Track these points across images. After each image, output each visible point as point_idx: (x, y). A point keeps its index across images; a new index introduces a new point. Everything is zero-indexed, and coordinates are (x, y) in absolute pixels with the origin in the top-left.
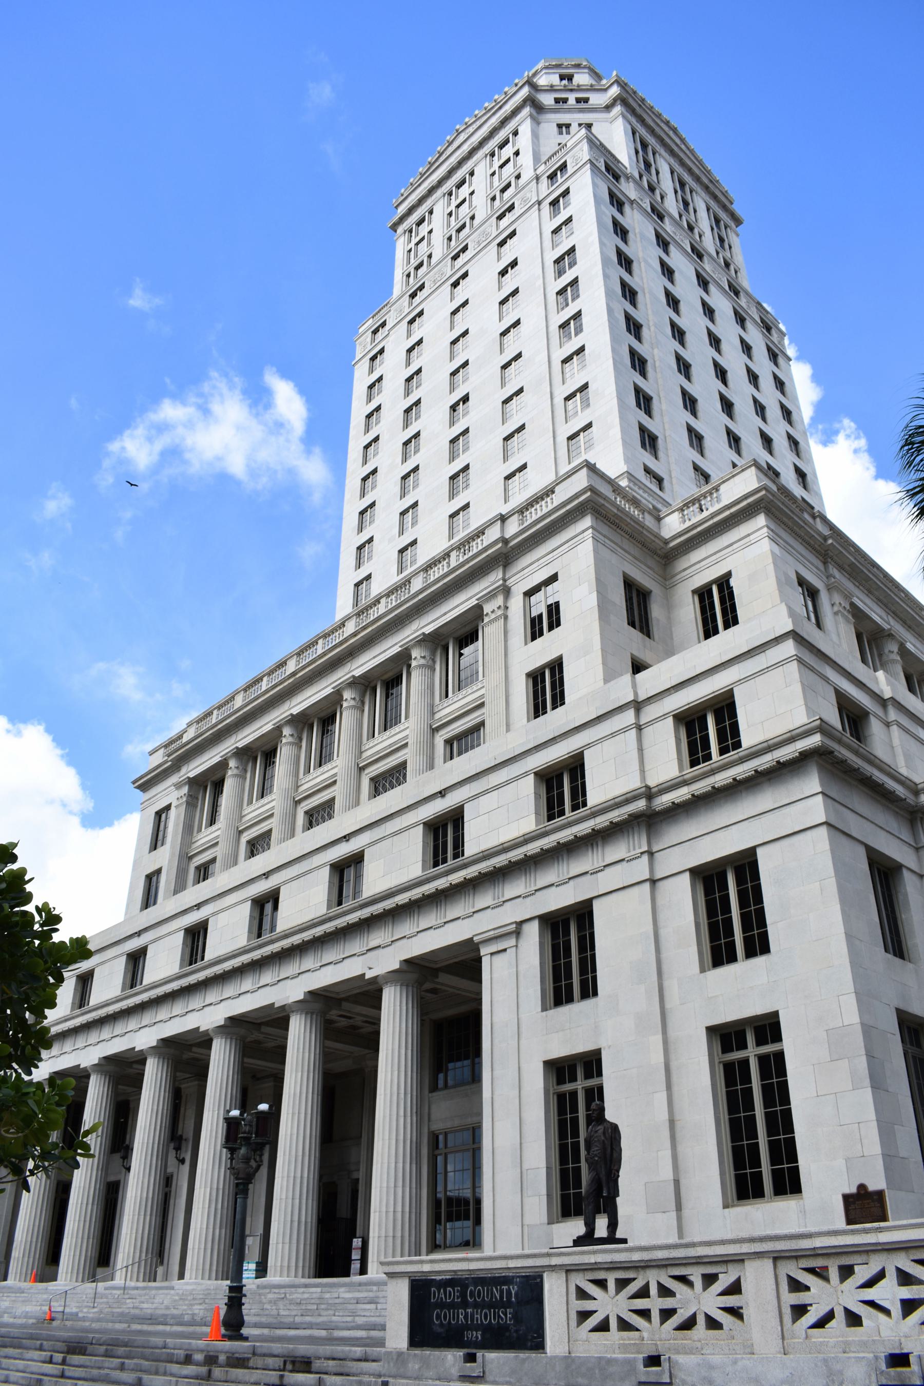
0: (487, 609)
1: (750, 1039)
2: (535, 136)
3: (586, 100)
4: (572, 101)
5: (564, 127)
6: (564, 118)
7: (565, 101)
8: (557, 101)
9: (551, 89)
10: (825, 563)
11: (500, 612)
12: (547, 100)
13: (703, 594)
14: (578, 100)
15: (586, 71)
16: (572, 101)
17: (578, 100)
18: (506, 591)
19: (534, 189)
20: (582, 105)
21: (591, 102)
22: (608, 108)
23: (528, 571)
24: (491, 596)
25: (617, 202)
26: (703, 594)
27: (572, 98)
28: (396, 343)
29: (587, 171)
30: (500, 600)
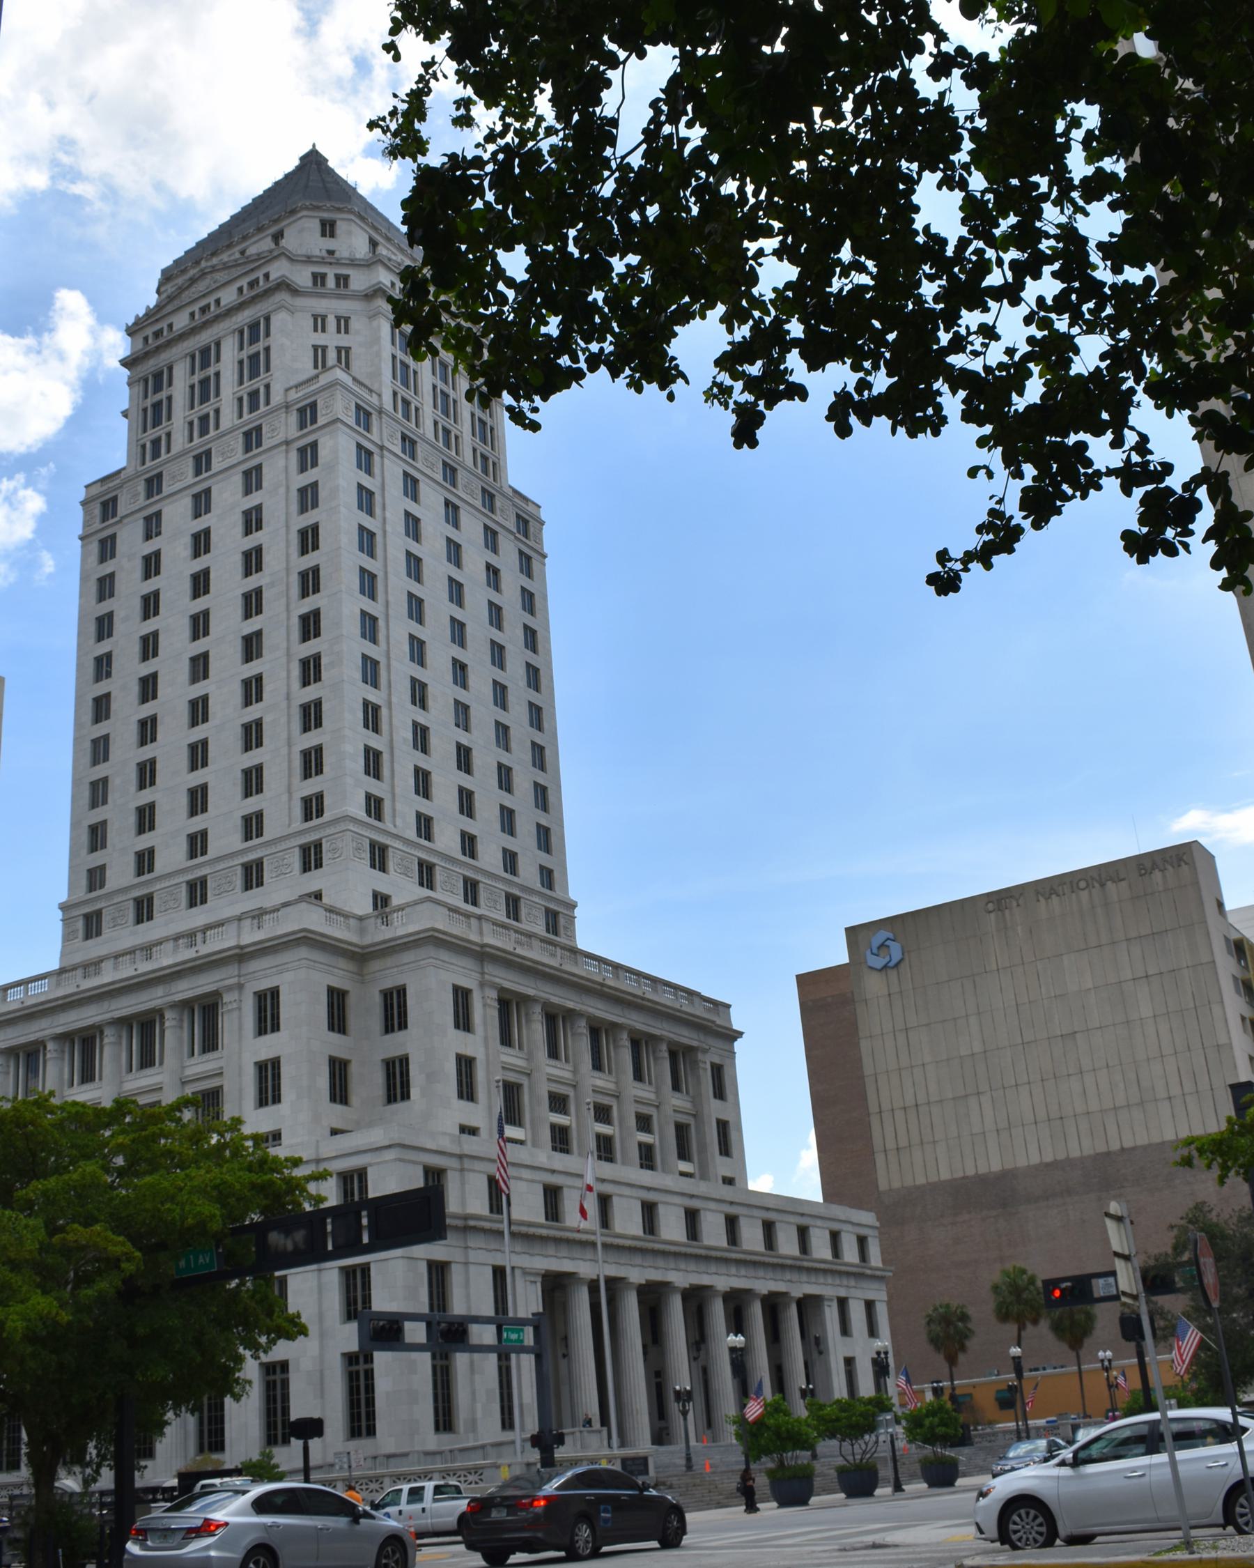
1: (361, 1360)
3: (346, 278)
4: (331, 282)
5: (319, 322)
6: (321, 305)
7: (323, 277)
8: (315, 276)
9: (309, 260)
10: (482, 961)
11: (235, 1005)
12: (302, 277)
14: (338, 277)
16: (331, 282)
18: (240, 987)
19: (283, 420)
20: (342, 291)
24: (230, 988)
27: (331, 273)
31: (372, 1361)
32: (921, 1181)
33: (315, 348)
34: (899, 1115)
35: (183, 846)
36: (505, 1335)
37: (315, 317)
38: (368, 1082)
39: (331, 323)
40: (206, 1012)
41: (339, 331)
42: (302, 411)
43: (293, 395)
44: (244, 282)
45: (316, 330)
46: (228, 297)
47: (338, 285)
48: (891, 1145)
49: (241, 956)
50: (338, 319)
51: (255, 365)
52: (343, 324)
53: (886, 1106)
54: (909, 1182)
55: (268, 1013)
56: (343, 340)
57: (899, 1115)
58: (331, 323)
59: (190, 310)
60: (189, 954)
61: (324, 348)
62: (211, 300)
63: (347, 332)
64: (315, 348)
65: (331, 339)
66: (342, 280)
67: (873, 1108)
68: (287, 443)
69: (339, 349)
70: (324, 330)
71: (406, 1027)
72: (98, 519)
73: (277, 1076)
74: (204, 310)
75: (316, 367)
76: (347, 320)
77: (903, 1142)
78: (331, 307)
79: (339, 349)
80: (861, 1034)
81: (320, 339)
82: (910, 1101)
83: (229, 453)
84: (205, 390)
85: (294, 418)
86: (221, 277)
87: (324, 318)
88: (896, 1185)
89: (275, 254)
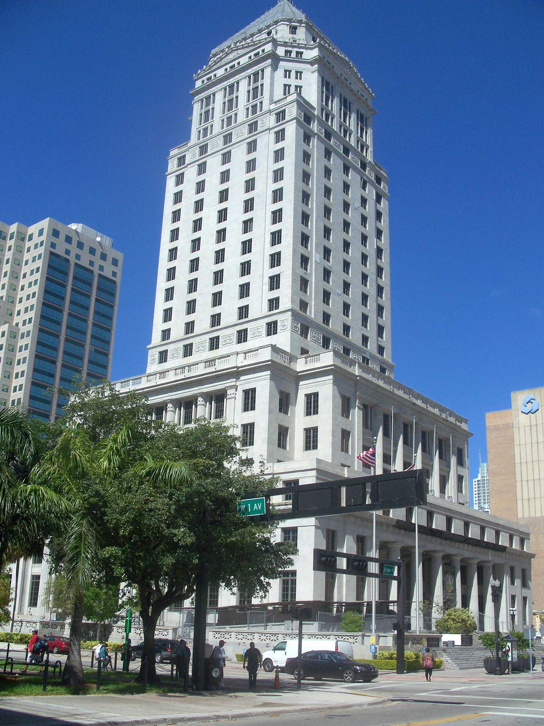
0: (229, 392)
2: (272, 78)
3: (301, 53)
4: (293, 55)
5: (287, 73)
7: (290, 52)
8: (286, 52)
9: (285, 44)
11: (233, 396)
12: (281, 51)
13: (308, 396)
14: (297, 53)
15: (304, 25)
16: (293, 55)
17: (297, 53)
18: (236, 387)
21: (304, 56)
22: (312, 63)
23: (245, 383)
24: (231, 387)
25: (307, 138)
26: (308, 396)
28: (191, 175)
29: (294, 124)
30: (233, 391)
31: (296, 576)
32: (538, 514)
33: (285, 86)
34: (531, 483)
35: (209, 321)
36: (385, 569)
37: (286, 71)
38: (297, 438)
39: (293, 74)
40: (219, 398)
41: (297, 78)
42: (278, 114)
43: (273, 107)
44: (252, 54)
45: (285, 77)
46: (244, 60)
47: (297, 56)
48: (525, 497)
49: (237, 373)
50: (297, 72)
51: (255, 93)
52: (299, 74)
53: (525, 478)
54: (533, 515)
55: (249, 400)
56: (298, 83)
57: (531, 483)
58: (293, 74)
59: (225, 67)
60: (212, 369)
61: (290, 86)
62: (236, 62)
63: (300, 79)
64: (285, 86)
65: (293, 81)
66: (299, 54)
67: (518, 478)
68: (270, 129)
69: (296, 87)
70: (289, 77)
71: (317, 413)
72: (176, 166)
73: (252, 433)
74: (231, 67)
75: (285, 94)
76: (301, 73)
77: (532, 496)
78: (294, 66)
79: (296, 87)
80: (515, 443)
81: (287, 81)
82: (536, 477)
83: (241, 133)
84: (230, 104)
85: (273, 118)
86: (241, 52)
87: (290, 72)
88: (526, 516)
89: (268, 40)
